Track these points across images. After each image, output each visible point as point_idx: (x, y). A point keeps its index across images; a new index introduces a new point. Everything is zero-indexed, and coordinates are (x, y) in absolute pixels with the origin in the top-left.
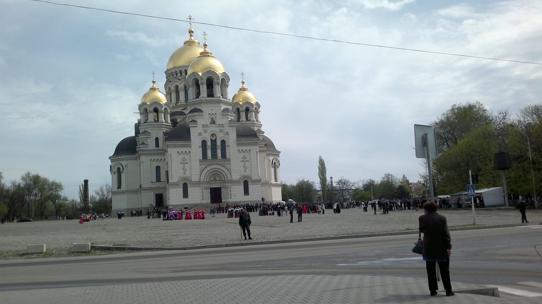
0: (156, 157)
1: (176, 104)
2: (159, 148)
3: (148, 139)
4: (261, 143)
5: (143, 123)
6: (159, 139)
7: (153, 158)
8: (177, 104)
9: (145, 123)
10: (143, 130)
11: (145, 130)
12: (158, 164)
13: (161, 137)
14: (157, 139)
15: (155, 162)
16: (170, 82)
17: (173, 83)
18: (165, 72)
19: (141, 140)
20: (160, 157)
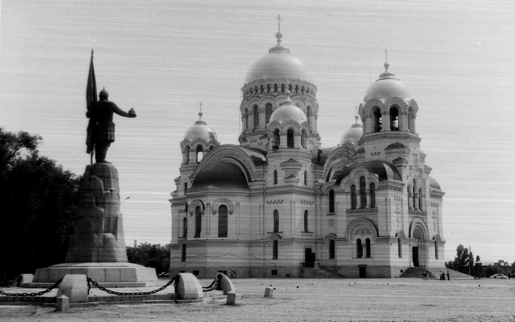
16: (248, 100)
18: (242, 88)
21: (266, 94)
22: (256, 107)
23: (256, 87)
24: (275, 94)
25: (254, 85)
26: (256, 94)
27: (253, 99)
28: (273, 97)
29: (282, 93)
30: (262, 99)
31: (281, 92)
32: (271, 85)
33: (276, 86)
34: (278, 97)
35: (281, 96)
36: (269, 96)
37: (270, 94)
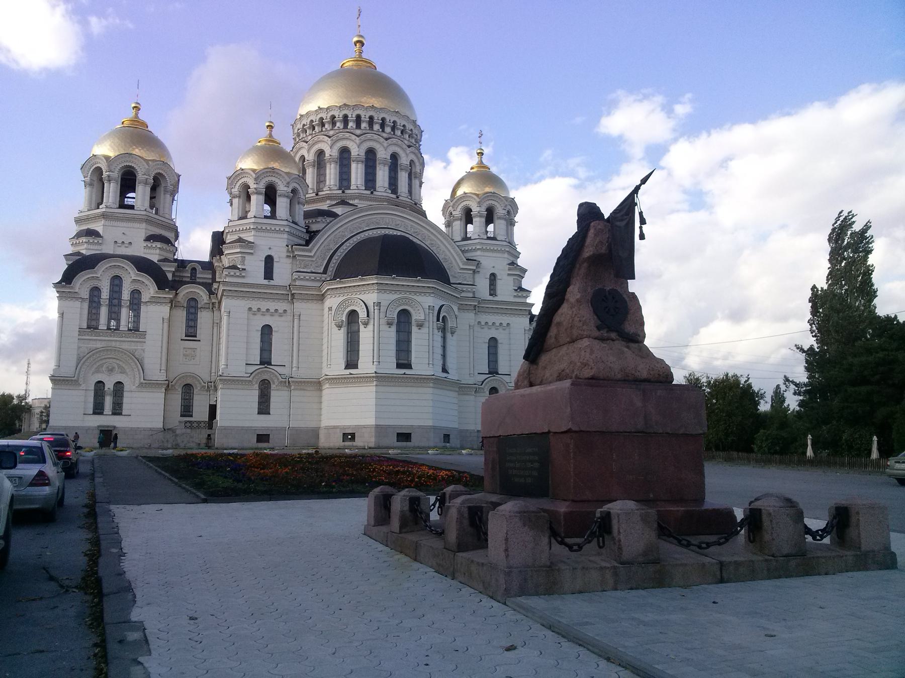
0: (264, 305)
1: (317, 195)
2: (272, 282)
3: (247, 257)
4: (520, 294)
5: (238, 220)
6: (275, 260)
7: (255, 305)
8: (320, 193)
9: (240, 219)
10: (235, 237)
11: (242, 236)
12: (268, 320)
13: (280, 253)
14: (269, 261)
15: (259, 316)
17: (314, 144)
19: (229, 259)
20: (272, 305)
21: (341, 130)
22: (321, 153)
23: (322, 119)
24: (358, 132)
25: (319, 116)
26: (322, 131)
27: (316, 139)
28: (354, 137)
29: (370, 132)
30: (334, 138)
31: (368, 128)
32: (350, 116)
33: (358, 117)
34: (362, 137)
35: (369, 136)
36: (347, 135)
37: (348, 130)
